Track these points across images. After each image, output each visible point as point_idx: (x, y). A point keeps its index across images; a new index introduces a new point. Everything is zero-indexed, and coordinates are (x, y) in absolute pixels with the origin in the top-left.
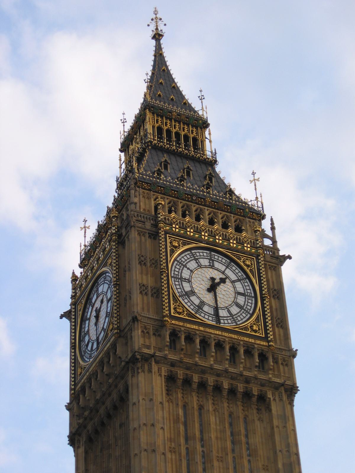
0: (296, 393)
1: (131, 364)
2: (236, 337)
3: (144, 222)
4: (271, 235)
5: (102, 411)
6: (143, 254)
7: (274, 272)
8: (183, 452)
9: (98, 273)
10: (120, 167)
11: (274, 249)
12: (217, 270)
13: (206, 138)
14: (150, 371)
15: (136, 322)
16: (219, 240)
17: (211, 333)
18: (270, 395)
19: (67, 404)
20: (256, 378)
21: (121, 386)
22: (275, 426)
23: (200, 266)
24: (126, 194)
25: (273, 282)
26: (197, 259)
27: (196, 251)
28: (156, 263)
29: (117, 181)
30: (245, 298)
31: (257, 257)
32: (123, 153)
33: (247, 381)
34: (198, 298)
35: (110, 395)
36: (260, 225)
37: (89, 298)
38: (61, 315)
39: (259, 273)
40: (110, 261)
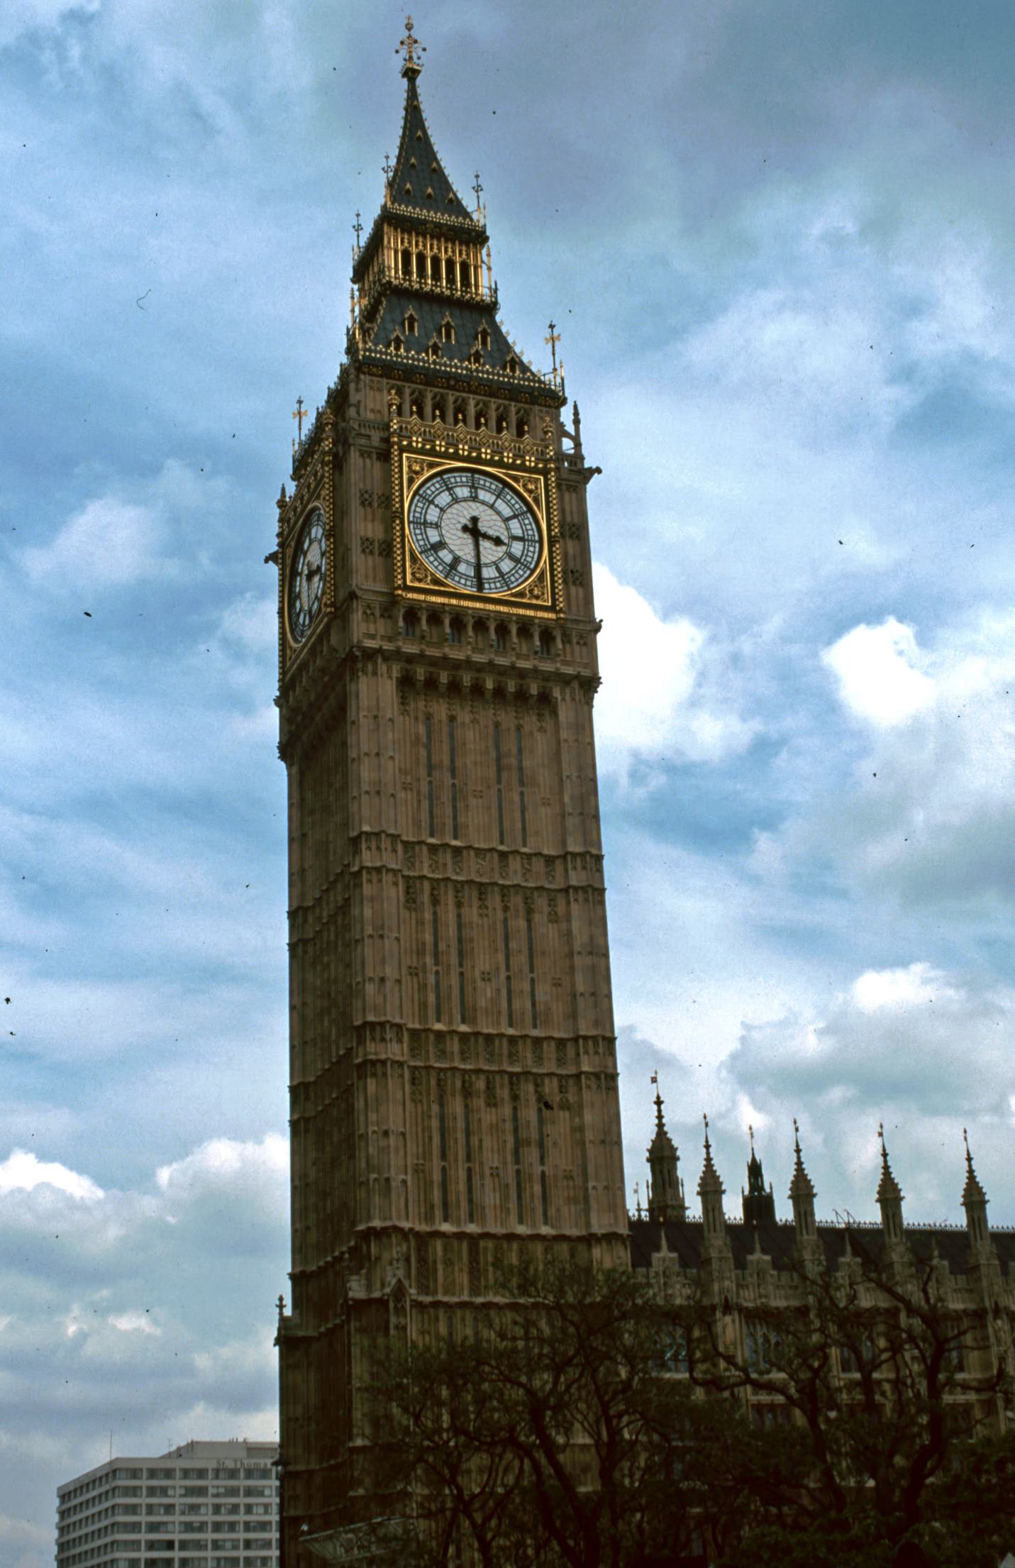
4: (573, 433)
6: (368, 488)
7: (574, 495)
8: (424, 788)
9: (310, 507)
10: (353, 311)
11: (578, 457)
12: (483, 503)
14: (375, 673)
16: (486, 453)
18: (556, 693)
20: (535, 670)
23: (456, 500)
25: (572, 513)
28: (387, 500)
33: (522, 674)
34: (451, 551)
35: (326, 699)
36: (559, 415)
37: (299, 543)
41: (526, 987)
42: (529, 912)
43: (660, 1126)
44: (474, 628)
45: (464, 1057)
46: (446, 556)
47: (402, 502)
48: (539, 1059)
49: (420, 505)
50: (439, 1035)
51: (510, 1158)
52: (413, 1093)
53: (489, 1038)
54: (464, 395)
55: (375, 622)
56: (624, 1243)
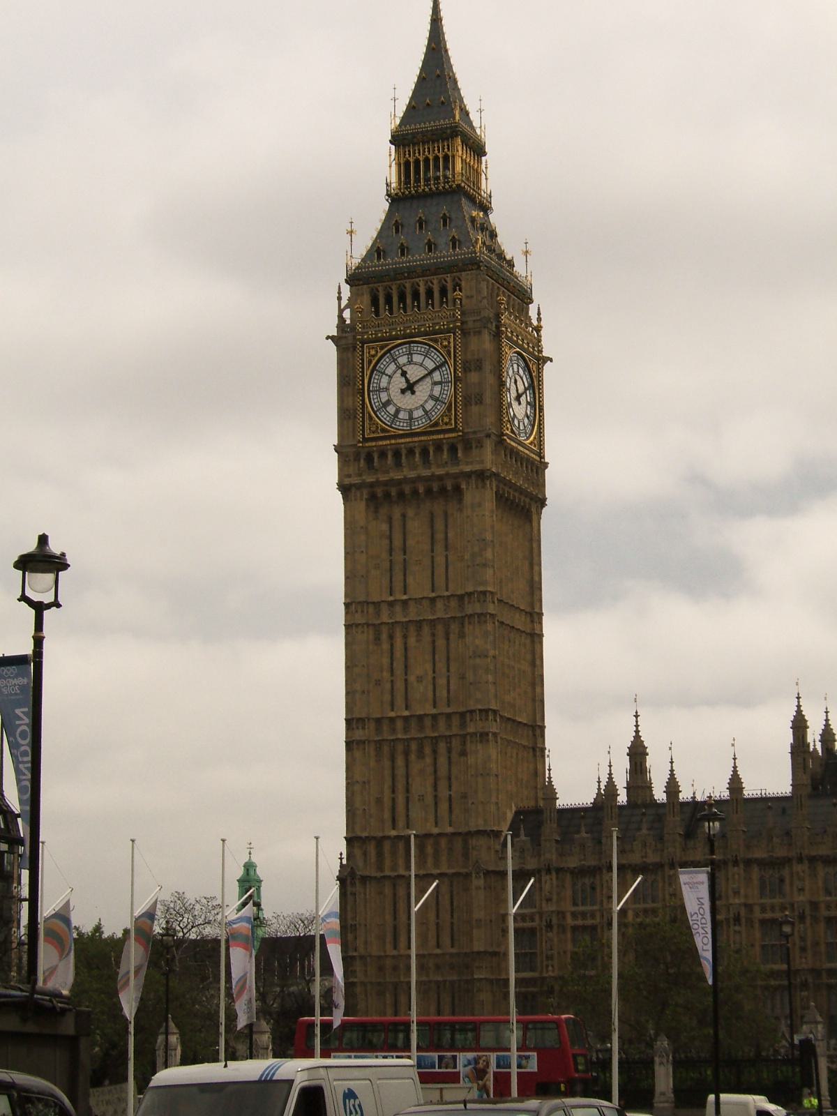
8: (387, 565)
17: (402, 443)
20: (447, 474)
33: (440, 478)
39: (455, 352)
41: (442, 682)
43: (637, 732)
44: (406, 455)
45: (406, 730)
46: (391, 409)
47: (363, 381)
48: (449, 726)
49: (377, 377)
50: (392, 720)
51: (430, 789)
52: (376, 756)
53: (421, 718)
54: (417, 280)
56: (489, 835)
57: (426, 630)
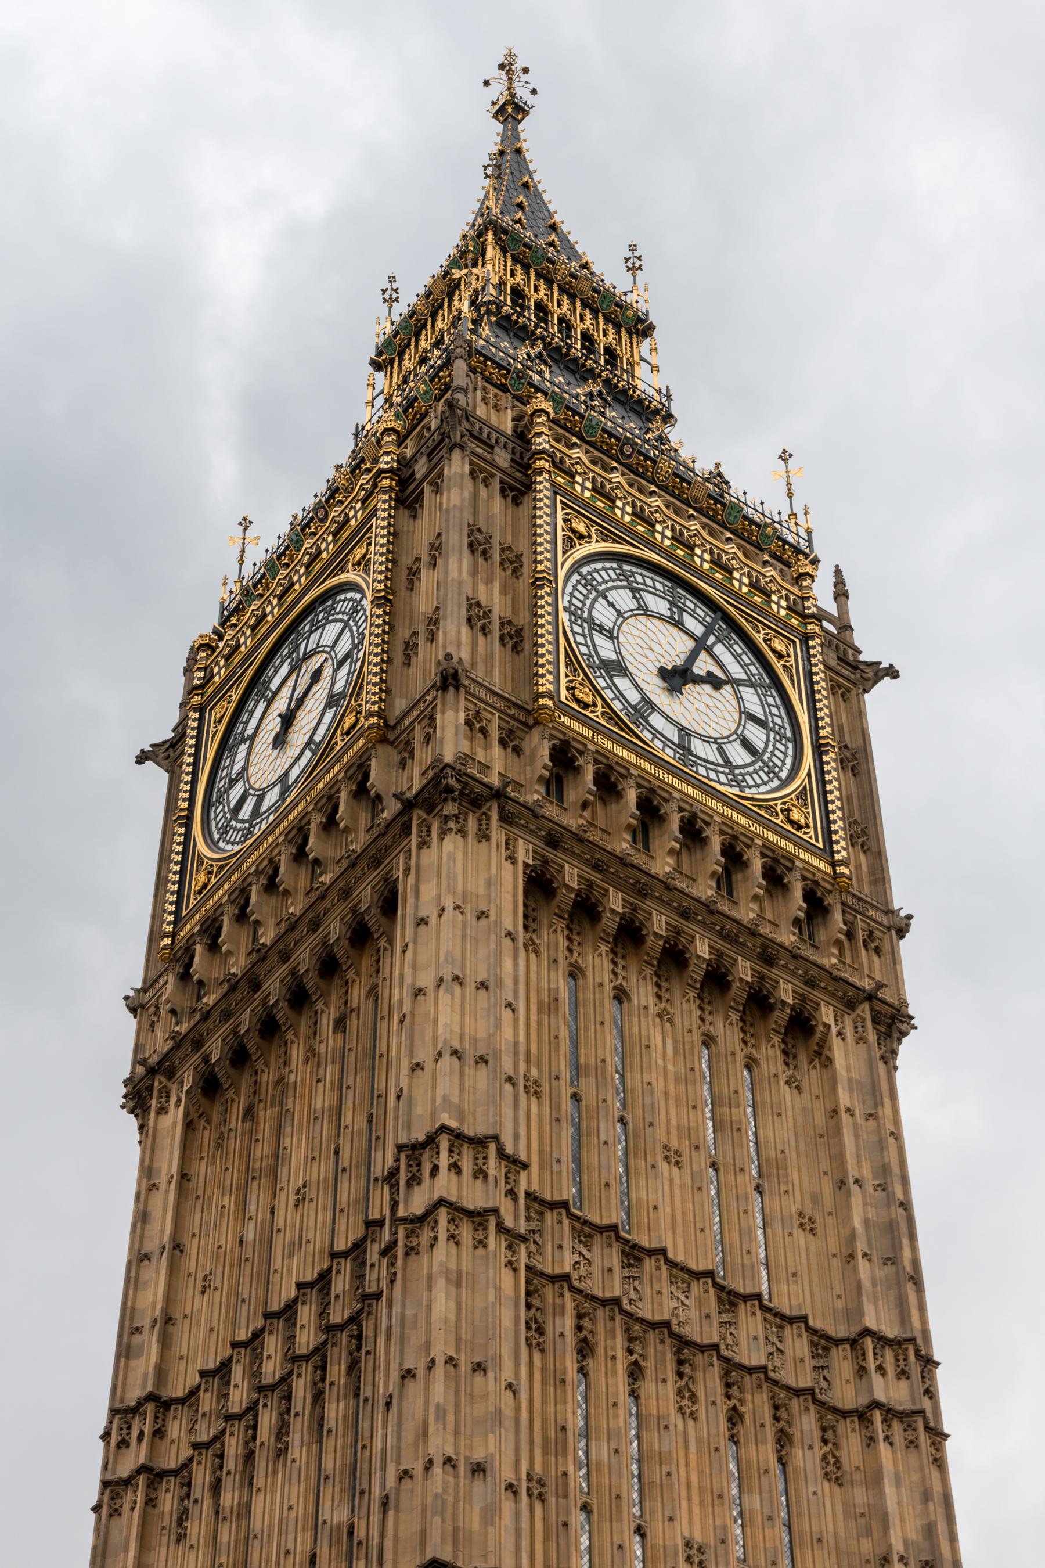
0: (905, 1034)
1: (417, 815)
2: (743, 821)
3: (492, 448)
4: (835, 613)
5: (274, 987)
13: (642, 359)
14: (484, 836)
15: (452, 689)
18: (827, 1014)
19: (132, 994)
21: (366, 895)
22: (843, 1109)
23: (644, 611)
24: (426, 392)
26: (638, 590)
27: (634, 569)
29: (357, 435)
30: (768, 736)
31: (806, 638)
32: (382, 374)
34: (637, 687)
38: (142, 751)
40: (359, 552)
42: (783, 1440)
55: (487, 747)
57: (709, 1382)
